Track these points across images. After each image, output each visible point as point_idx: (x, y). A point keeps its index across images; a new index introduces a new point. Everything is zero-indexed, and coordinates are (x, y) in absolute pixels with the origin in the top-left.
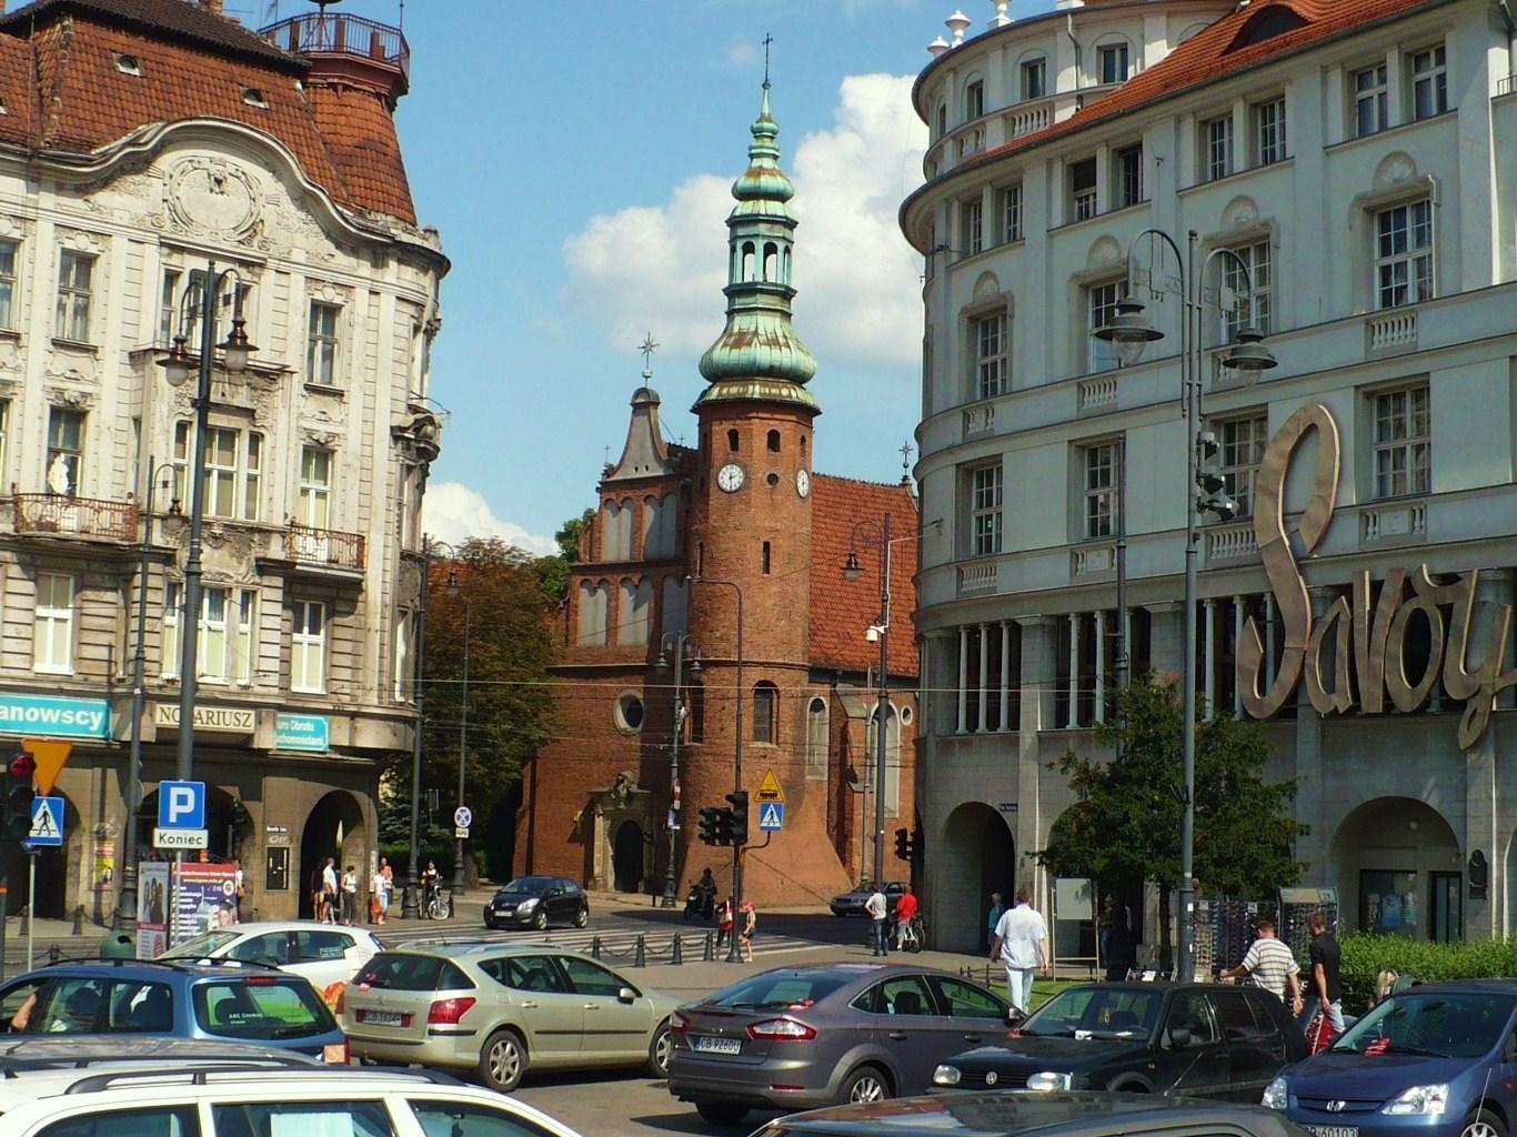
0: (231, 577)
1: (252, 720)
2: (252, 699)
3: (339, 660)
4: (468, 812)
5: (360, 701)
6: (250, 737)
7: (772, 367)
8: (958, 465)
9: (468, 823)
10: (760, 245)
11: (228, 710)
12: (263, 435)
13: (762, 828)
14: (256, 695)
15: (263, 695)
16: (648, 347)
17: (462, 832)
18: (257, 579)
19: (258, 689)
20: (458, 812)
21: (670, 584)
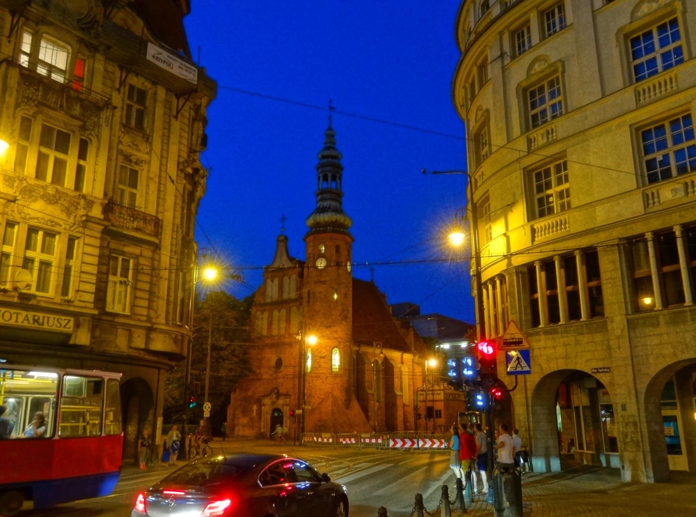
0: (60, 225)
1: (71, 324)
2: (72, 309)
3: (139, 294)
4: (210, 405)
5: (154, 320)
6: (68, 336)
7: (337, 220)
8: (524, 169)
9: (209, 410)
10: (330, 175)
11: (52, 316)
12: (91, 140)
13: (509, 373)
14: (75, 306)
15: (82, 307)
16: (283, 219)
17: (207, 414)
18: (81, 230)
19: (77, 303)
20: (205, 405)
21: (294, 309)
